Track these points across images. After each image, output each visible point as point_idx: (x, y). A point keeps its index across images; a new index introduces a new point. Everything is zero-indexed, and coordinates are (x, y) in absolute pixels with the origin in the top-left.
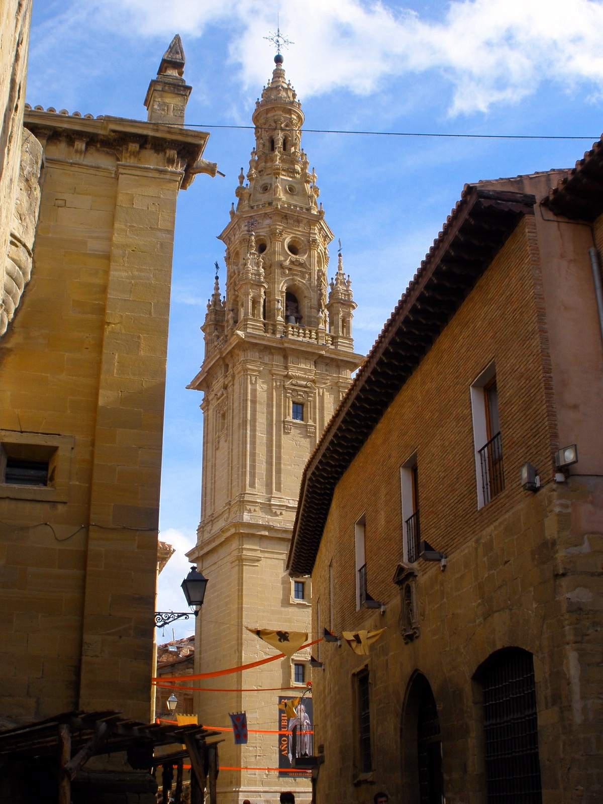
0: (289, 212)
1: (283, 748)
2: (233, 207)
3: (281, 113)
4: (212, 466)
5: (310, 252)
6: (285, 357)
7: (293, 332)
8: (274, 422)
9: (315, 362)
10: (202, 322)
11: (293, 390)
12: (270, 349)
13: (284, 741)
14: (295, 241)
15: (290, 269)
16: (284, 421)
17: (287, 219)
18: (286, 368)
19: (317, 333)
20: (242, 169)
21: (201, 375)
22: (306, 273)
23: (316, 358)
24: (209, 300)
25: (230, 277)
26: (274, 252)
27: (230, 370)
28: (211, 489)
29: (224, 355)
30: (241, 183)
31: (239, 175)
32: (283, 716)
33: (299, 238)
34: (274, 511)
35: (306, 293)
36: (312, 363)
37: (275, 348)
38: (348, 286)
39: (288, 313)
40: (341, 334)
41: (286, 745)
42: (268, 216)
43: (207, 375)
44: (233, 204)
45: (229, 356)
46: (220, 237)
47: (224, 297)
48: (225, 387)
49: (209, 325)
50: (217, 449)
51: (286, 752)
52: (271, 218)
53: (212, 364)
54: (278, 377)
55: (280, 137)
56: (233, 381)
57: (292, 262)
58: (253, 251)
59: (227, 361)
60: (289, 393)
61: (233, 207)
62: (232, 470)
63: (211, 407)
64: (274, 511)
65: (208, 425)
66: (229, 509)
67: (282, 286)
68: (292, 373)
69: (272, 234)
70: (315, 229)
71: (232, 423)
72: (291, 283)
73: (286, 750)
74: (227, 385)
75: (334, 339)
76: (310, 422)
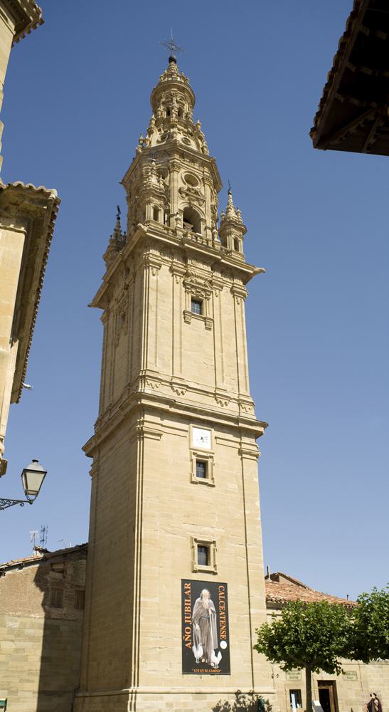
1: (186, 640)
6: (185, 260)
11: (193, 287)
12: (171, 249)
13: (188, 630)
15: (187, 195)
16: (184, 312)
23: (212, 262)
25: (131, 208)
27: (132, 270)
28: (110, 384)
29: (126, 257)
32: (187, 602)
34: (175, 389)
41: (189, 636)
43: (108, 287)
45: (130, 259)
46: (121, 183)
48: (127, 288)
49: (111, 251)
50: (116, 346)
51: (190, 643)
53: (114, 270)
59: (128, 264)
62: (132, 355)
64: (175, 389)
73: (189, 642)
74: (128, 285)
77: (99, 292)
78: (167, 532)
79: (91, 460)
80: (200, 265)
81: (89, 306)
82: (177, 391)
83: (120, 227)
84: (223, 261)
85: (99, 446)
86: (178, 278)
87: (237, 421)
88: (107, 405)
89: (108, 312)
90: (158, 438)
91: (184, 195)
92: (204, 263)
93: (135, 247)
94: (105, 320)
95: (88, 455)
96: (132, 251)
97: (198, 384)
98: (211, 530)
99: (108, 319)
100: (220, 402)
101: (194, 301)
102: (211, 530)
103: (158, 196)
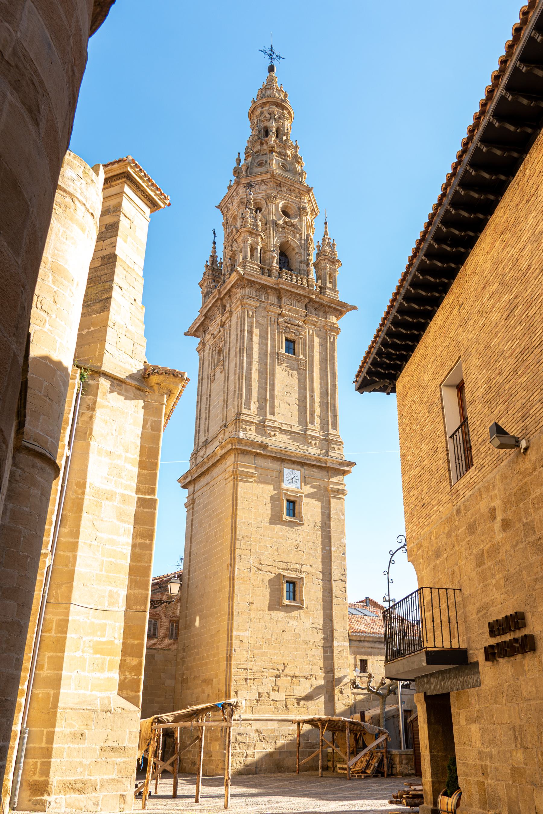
0: (283, 181)
2: (231, 183)
3: (275, 107)
4: (207, 398)
5: (300, 217)
7: (287, 277)
8: (269, 353)
9: (306, 305)
10: (200, 278)
11: (286, 327)
14: (288, 206)
15: (283, 228)
17: (281, 187)
18: (280, 307)
19: (308, 283)
20: (239, 153)
21: (200, 319)
22: (298, 233)
23: (307, 301)
24: (207, 261)
25: (228, 236)
26: (270, 213)
27: (228, 309)
29: (222, 295)
30: (239, 164)
31: (237, 157)
33: (291, 205)
34: (268, 432)
37: (271, 288)
38: (334, 248)
39: (282, 267)
40: (328, 286)
42: (264, 182)
43: (204, 319)
44: (231, 181)
45: (227, 297)
46: (217, 207)
47: (221, 259)
48: (222, 326)
52: (266, 185)
55: (274, 126)
56: (231, 317)
57: (285, 223)
58: (252, 207)
59: (224, 301)
60: (283, 329)
61: (231, 183)
63: (207, 347)
64: (268, 432)
65: (203, 364)
66: (224, 430)
67: (275, 241)
69: (268, 198)
70: (304, 199)
71: (229, 354)
72: (285, 240)
74: (224, 323)
75: (322, 289)
76: (301, 357)
77: (195, 323)
79: (186, 492)
81: (186, 334)
83: (215, 252)
85: (195, 480)
88: (202, 439)
89: (203, 344)
93: (232, 287)
94: (201, 350)
95: (184, 487)
96: (229, 290)
99: (204, 351)
101: (287, 340)
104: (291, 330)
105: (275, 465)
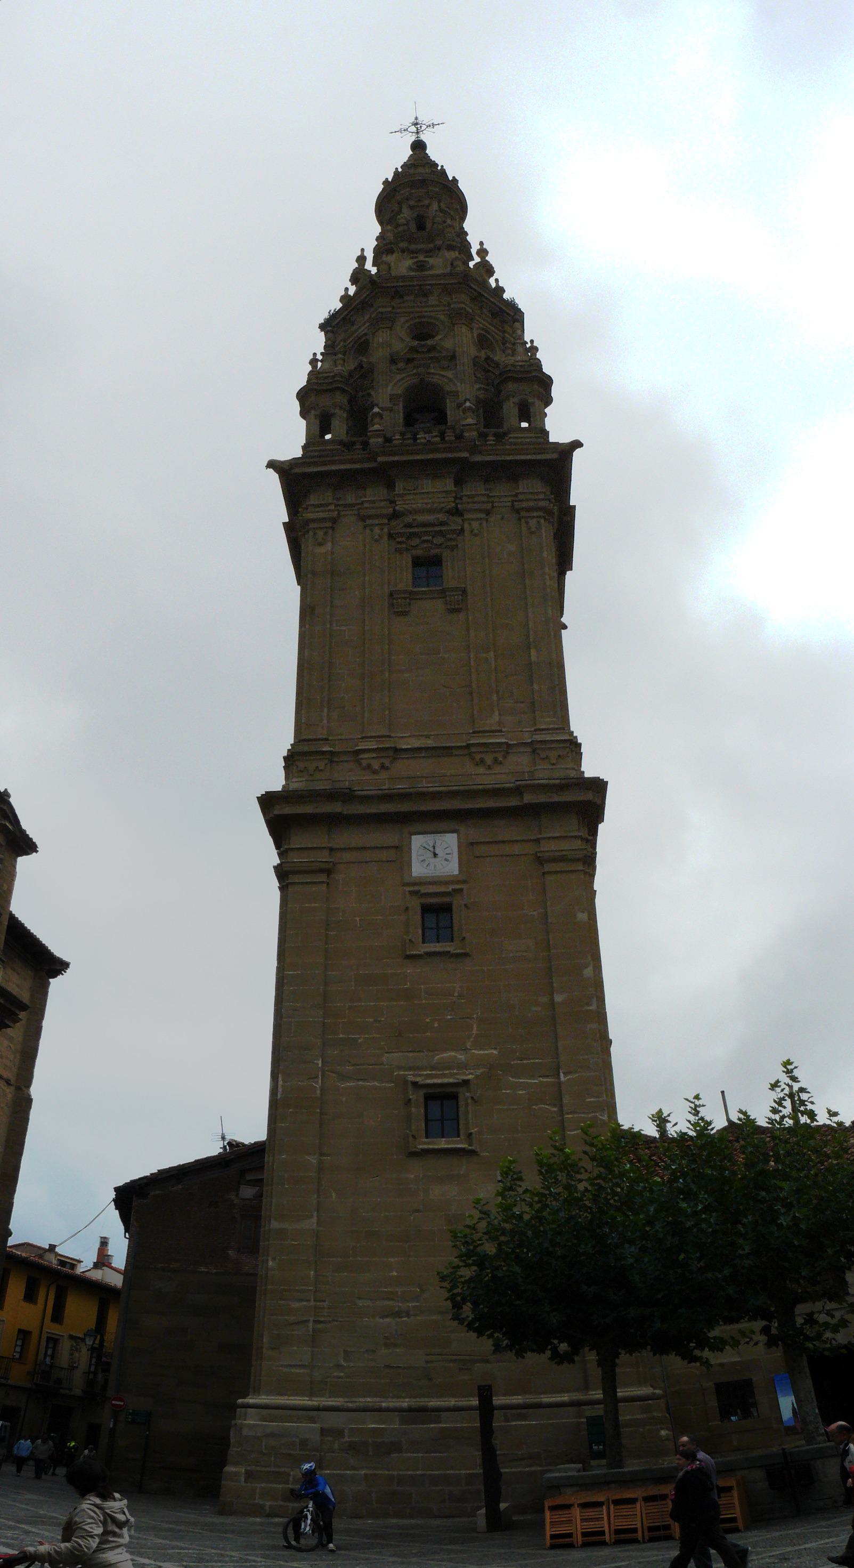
6: (391, 486)
11: (411, 536)
17: (401, 297)
18: (393, 502)
34: (364, 763)
35: (447, 388)
36: (449, 484)
54: (376, 522)
68: (404, 506)
72: (416, 380)
78: (343, 1077)
80: (428, 486)
82: (369, 766)
84: (478, 458)
86: (377, 531)
87: (518, 791)
90: (322, 878)
91: (401, 365)
92: (435, 477)
97: (427, 737)
98: (461, 1057)
100: (482, 761)
102: (461, 1057)
103: (327, 390)
104: (423, 538)
105: (386, 837)
